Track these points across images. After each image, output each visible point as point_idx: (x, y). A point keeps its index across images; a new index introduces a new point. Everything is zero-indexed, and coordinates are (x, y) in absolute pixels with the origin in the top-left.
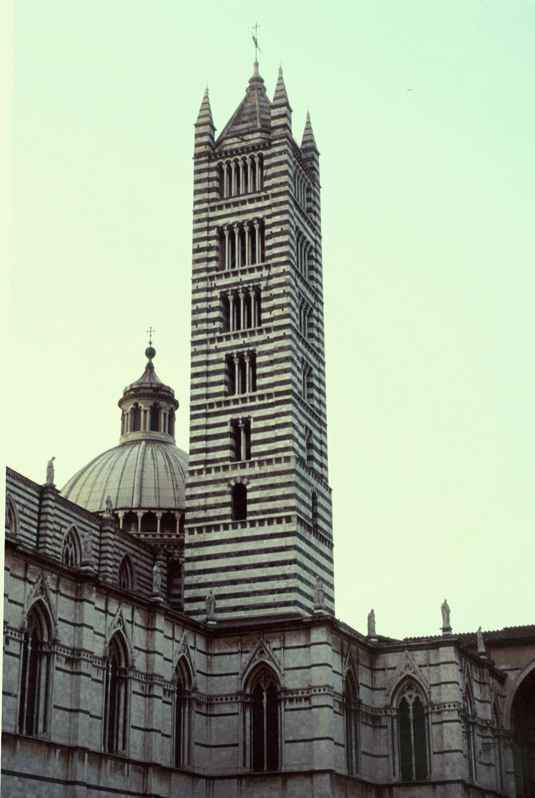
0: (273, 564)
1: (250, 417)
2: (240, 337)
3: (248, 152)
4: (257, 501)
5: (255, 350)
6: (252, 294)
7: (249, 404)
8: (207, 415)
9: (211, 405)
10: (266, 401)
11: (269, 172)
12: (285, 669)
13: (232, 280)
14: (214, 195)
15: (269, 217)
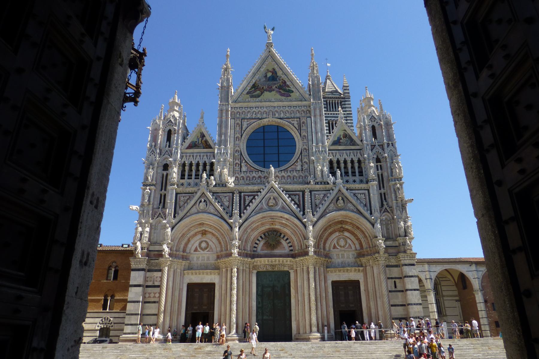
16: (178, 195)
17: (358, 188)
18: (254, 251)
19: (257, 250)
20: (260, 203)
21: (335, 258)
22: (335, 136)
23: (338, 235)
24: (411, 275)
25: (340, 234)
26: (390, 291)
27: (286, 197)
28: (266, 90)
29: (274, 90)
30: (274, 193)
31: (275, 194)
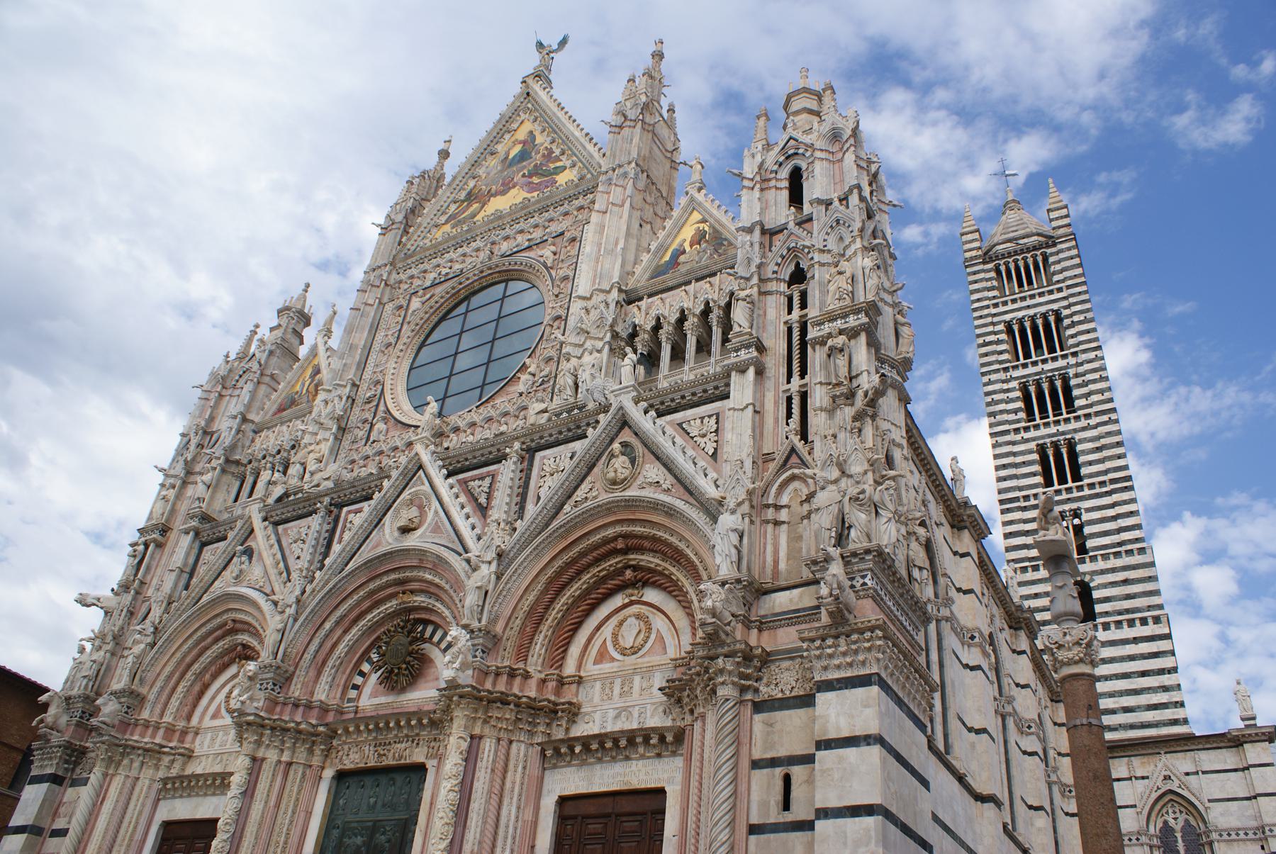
0: (1144, 674)
1: (1079, 509)
2: (1052, 425)
3: (1028, 252)
4: (1107, 600)
5: (1073, 438)
6: (1058, 383)
7: (1076, 494)
8: (1024, 509)
9: (1026, 498)
10: (1098, 490)
11: (1058, 267)
12: (1210, 801)
13: (1031, 370)
14: (995, 293)
15: (1068, 307)
16: (206, 548)
17: (694, 394)
18: (350, 700)
19: (359, 696)
20: (376, 526)
21: (597, 699)
22: (662, 249)
23: (620, 604)
24: (845, 734)
25: (627, 601)
26: (754, 829)
27: (443, 486)
28: (495, 195)
29: (514, 187)
30: (423, 484)
31: (427, 487)
